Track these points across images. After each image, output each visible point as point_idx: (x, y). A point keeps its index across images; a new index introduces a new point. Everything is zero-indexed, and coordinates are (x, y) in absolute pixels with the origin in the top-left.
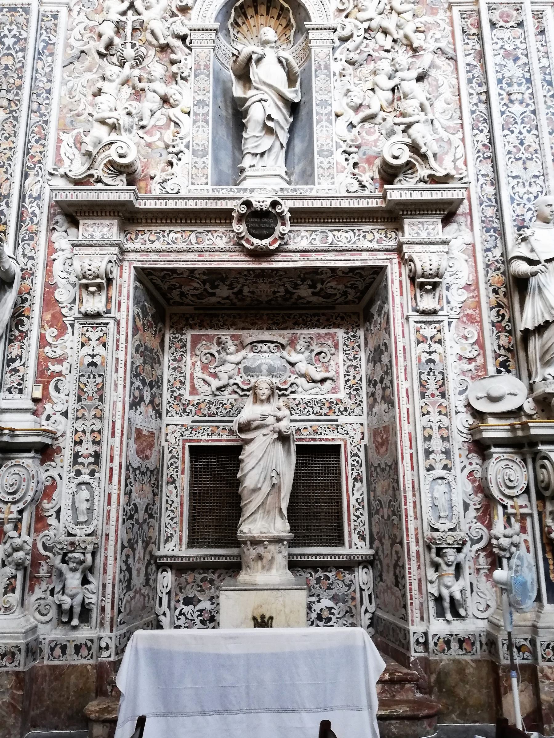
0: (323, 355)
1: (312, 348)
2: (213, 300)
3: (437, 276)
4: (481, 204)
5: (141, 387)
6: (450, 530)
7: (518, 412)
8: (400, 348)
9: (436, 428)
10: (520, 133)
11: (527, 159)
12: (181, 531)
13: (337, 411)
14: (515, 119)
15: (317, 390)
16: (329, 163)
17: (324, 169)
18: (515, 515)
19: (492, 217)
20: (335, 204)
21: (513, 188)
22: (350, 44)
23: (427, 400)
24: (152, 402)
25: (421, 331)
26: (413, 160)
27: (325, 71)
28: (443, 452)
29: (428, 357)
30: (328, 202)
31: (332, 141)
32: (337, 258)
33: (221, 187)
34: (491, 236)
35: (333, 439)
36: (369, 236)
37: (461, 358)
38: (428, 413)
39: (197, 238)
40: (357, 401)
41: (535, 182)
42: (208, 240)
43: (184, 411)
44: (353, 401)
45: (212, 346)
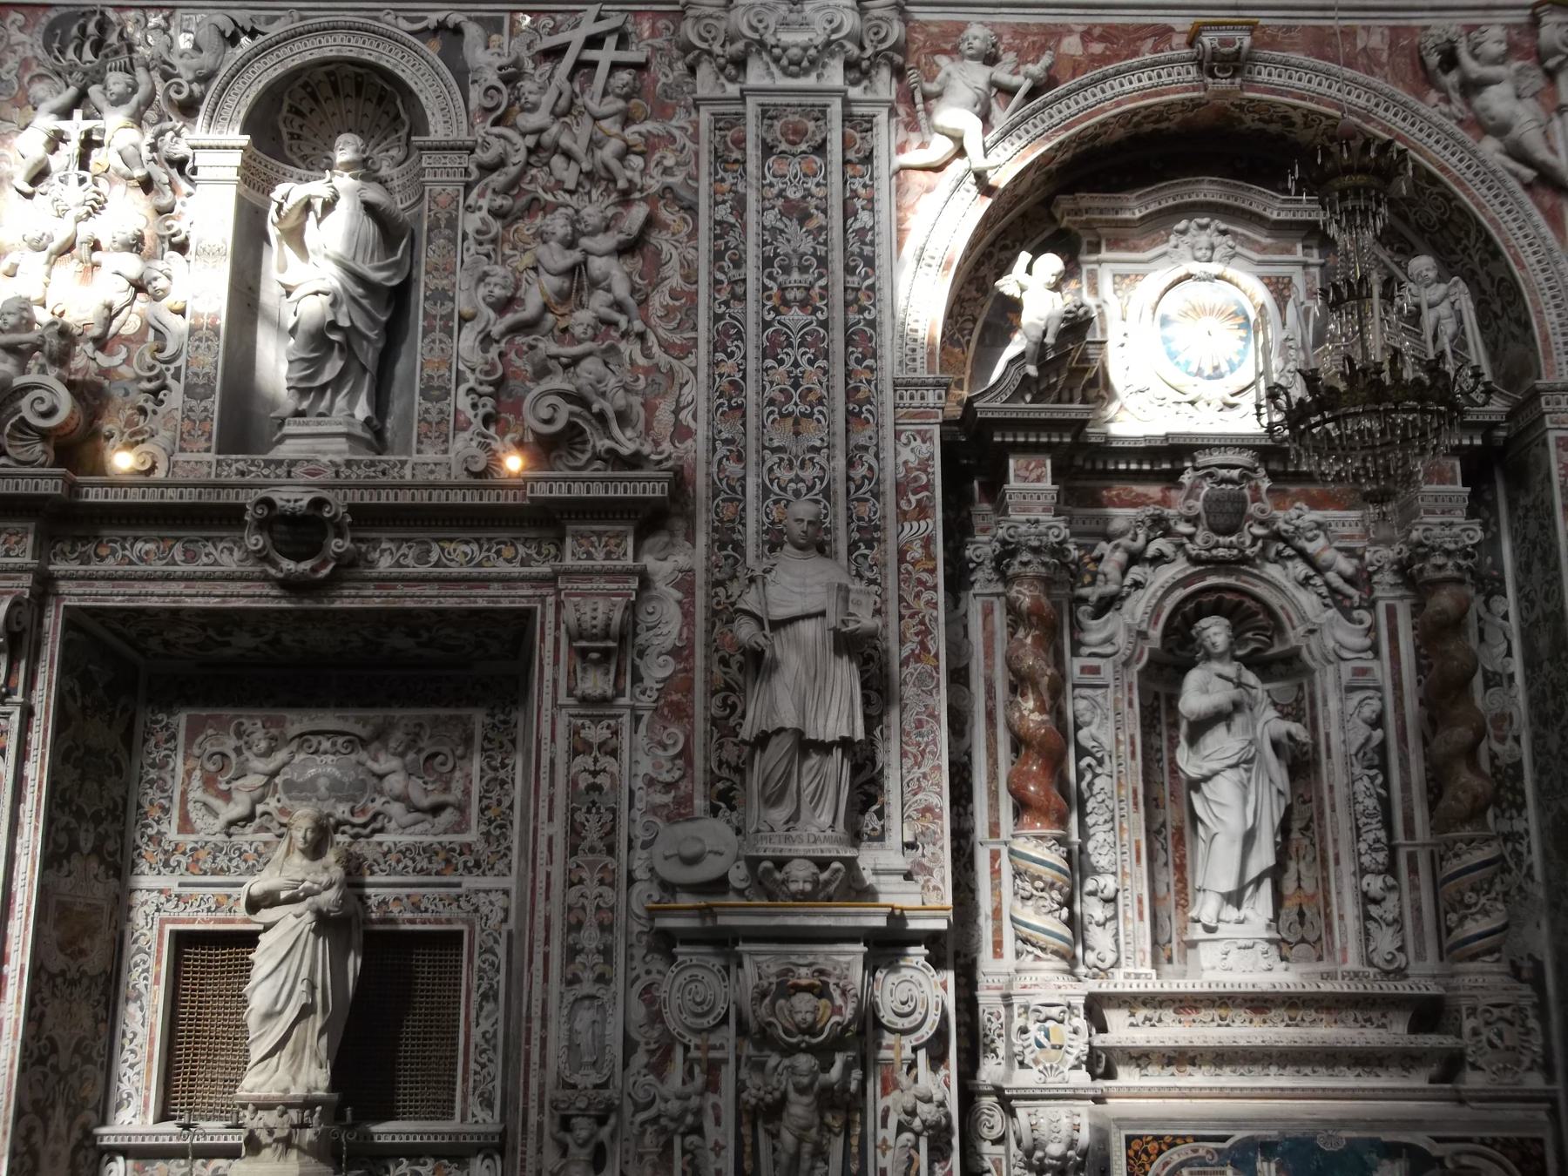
0: (440, 758)
1: (422, 745)
2: (228, 652)
3: (606, 636)
4: (715, 497)
5: (74, 824)
6: (596, 1087)
7: (720, 885)
8: (545, 761)
9: (591, 909)
10: (796, 364)
11: (803, 414)
12: (148, 1088)
13: (460, 866)
14: (788, 337)
15: (427, 826)
16: (441, 411)
17: (430, 423)
18: (698, 1061)
19: (733, 521)
20: (438, 498)
21: (771, 470)
22: (498, 179)
23: (580, 859)
24: (97, 850)
25: (583, 733)
26: (580, 422)
27: (447, 232)
28: (599, 952)
29: (591, 780)
30: (426, 494)
31: (450, 370)
32: (443, 592)
33: (234, 457)
34: (727, 557)
35: (449, 921)
36: (508, 552)
37: (651, 782)
38: (581, 881)
39: (186, 552)
40: (501, 848)
41: (811, 459)
42: (207, 555)
43: (166, 864)
44: (493, 848)
45: (225, 739)
